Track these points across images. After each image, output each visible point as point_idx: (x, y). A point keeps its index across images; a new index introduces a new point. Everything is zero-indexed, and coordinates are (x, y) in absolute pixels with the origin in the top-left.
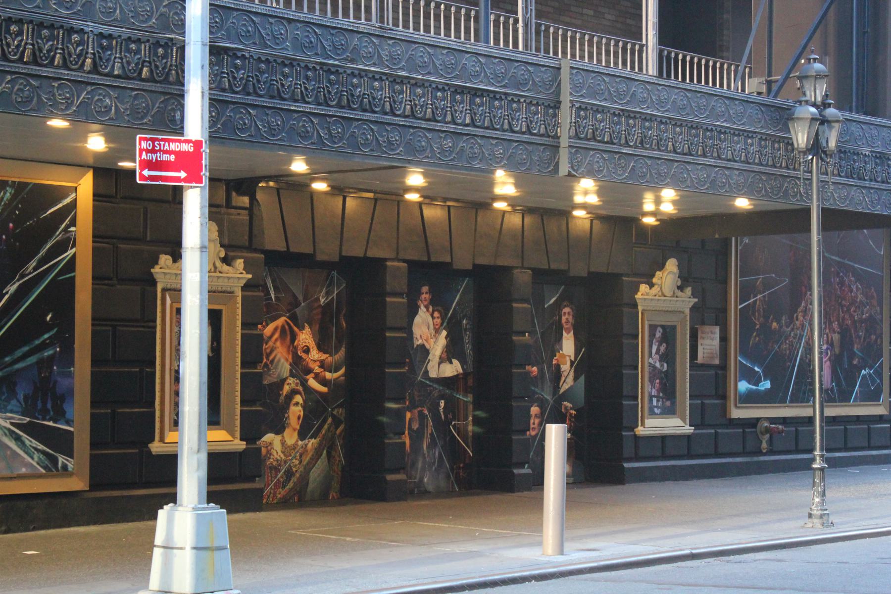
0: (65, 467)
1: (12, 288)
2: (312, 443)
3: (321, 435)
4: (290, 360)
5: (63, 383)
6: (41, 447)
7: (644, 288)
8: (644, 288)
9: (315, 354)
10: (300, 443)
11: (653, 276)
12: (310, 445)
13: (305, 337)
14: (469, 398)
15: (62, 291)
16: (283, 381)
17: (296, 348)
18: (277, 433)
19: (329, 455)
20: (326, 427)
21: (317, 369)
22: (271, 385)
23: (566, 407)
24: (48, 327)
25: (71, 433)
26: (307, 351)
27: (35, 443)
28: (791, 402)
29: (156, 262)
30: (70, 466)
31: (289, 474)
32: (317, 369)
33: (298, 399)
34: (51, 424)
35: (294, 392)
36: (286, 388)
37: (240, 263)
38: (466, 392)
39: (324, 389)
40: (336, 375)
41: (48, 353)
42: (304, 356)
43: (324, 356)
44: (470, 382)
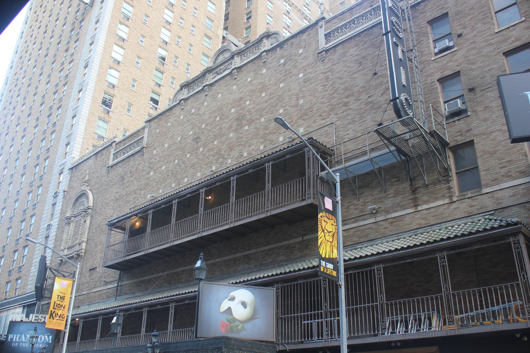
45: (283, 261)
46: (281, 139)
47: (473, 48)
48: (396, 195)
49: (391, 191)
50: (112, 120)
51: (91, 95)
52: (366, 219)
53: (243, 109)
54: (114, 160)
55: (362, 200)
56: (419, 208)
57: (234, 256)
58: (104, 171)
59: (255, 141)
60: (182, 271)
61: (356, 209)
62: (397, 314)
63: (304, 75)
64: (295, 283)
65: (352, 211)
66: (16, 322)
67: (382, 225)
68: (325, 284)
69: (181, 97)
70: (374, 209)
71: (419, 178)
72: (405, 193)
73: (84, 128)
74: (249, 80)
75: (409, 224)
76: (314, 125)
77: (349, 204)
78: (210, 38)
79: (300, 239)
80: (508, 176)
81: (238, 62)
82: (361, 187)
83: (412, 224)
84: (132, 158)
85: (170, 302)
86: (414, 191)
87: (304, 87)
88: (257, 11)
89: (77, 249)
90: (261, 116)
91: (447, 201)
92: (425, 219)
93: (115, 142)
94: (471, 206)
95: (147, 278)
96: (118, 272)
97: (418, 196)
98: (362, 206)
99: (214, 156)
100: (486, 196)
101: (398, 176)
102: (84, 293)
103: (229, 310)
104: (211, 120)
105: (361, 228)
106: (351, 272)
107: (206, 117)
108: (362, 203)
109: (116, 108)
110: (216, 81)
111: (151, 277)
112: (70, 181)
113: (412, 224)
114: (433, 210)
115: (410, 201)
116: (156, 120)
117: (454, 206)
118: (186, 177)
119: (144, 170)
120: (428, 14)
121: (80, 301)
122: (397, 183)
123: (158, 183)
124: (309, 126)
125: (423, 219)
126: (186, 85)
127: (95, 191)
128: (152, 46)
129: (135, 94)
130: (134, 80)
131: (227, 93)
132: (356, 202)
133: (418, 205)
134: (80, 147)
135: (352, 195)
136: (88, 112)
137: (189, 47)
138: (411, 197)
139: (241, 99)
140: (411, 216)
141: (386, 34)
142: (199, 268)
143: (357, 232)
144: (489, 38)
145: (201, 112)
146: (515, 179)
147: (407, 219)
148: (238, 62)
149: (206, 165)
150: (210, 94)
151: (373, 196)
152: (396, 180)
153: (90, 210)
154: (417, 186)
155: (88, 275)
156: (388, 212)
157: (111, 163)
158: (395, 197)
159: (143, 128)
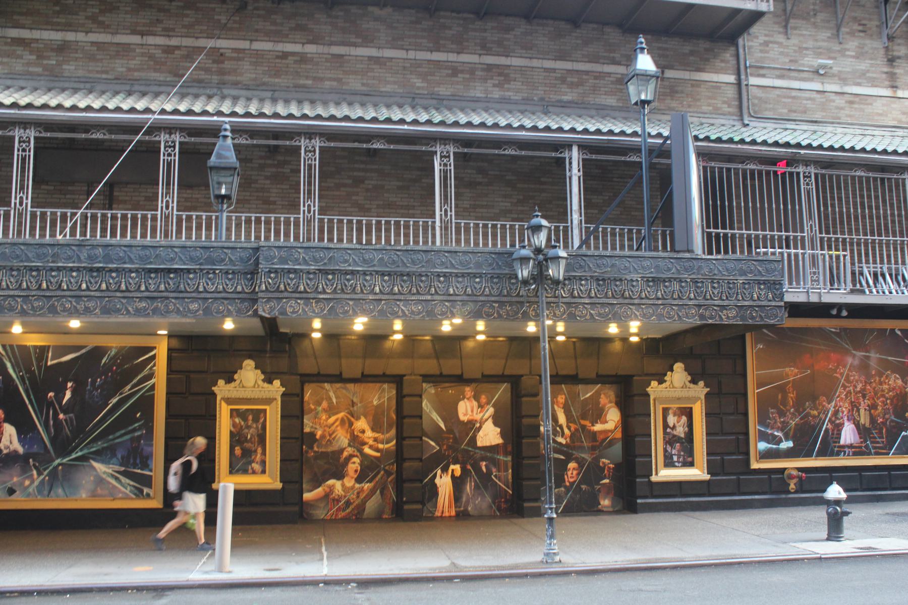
0: (148, 495)
1: (114, 400)
2: (367, 486)
3: (375, 481)
4: (349, 437)
5: (147, 449)
6: (132, 483)
7: (654, 384)
8: (654, 384)
9: (369, 434)
10: (357, 486)
11: (666, 375)
12: (366, 487)
13: (361, 424)
14: (509, 458)
15: (147, 402)
16: (342, 451)
17: (353, 431)
18: (338, 479)
19: (382, 493)
20: (379, 476)
21: (371, 442)
22: (333, 452)
23: (603, 463)
24: (138, 420)
25: (151, 476)
26: (363, 432)
27: (128, 481)
28: (817, 456)
29: (215, 384)
30: (152, 494)
31: (348, 503)
32: (371, 442)
33: (356, 460)
34: (139, 471)
35: (351, 456)
36: (345, 454)
37: (277, 383)
38: (506, 454)
39: (378, 454)
40: (387, 446)
41: (137, 434)
42: (360, 435)
43: (377, 435)
44: (510, 448)
45: (613, 108)
48: (860, 55)
49: (852, 45)
55: (794, 41)
57: (452, 57)
60: (235, 50)
61: (781, 53)
62: (882, 262)
64: (740, 166)
65: (771, 55)
67: (834, 101)
68: (808, 184)
70: (824, 67)
71: (899, 41)
72: (876, 59)
75: (881, 115)
77: (767, 39)
83: (887, 116)
85: (299, 134)
95: (56, 36)
97: (897, 71)
98: (795, 51)
101: (863, 22)
105: (794, 93)
106: (863, 174)
108: (794, 45)
111: (70, 36)
113: (887, 116)
115: (884, 76)
122: (862, 34)
125: (904, 113)
132: (781, 38)
133: (896, 87)
135: (775, 23)
138: (886, 70)
142: (645, 76)
143: (785, 97)
147: (878, 106)
151: (816, 40)
152: (861, 28)
154: (896, 53)
156: (844, 80)
158: (858, 58)
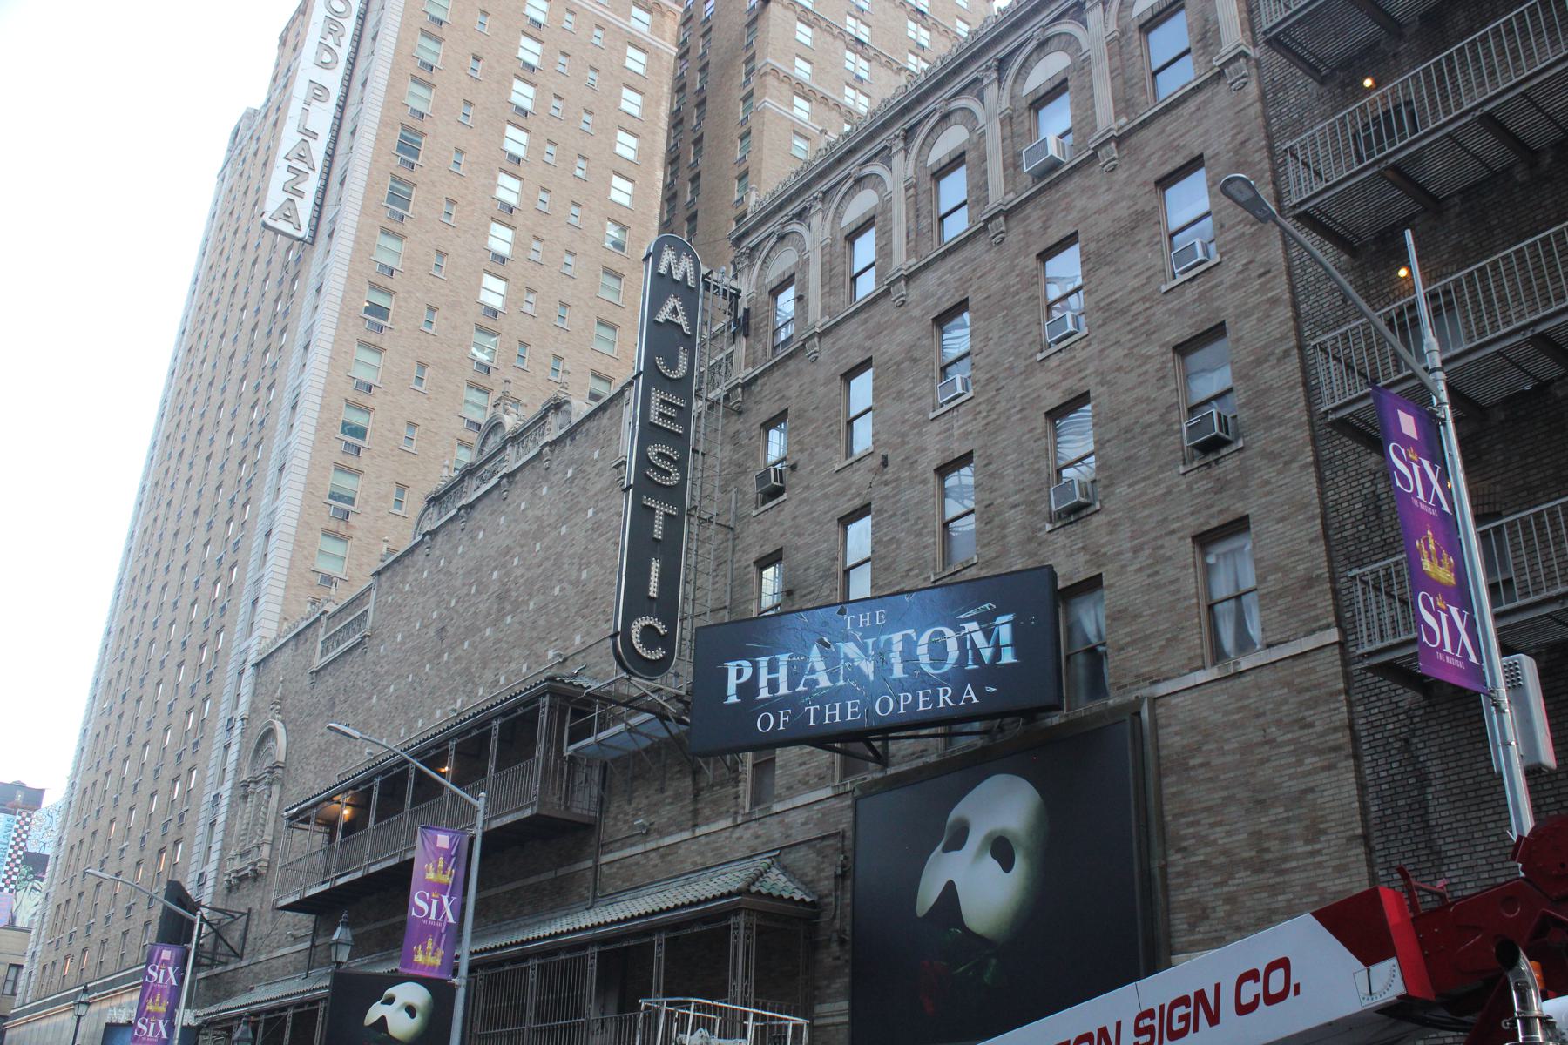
46: (551, 654)
47: (805, 501)
48: (677, 797)
50: (357, 534)
51: (303, 480)
52: (633, 845)
53: (508, 574)
54: (325, 652)
56: (698, 832)
58: (307, 681)
59: (516, 653)
63: (595, 513)
66: (117, 1025)
69: (428, 527)
73: (286, 563)
74: (523, 506)
76: (595, 631)
78: (619, 276)
79: (551, 875)
80: (806, 783)
81: (513, 459)
82: (634, 778)
84: (350, 658)
86: (696, 794)
87: (592, 541)
88: (759, 171)
89: (255, 859)
90: (531, 596)
91: (728, 822)
92: (701, 854)
93: (325, 612)
94: (757, 837)
96: (313, 917)
99: (460, 675)
100: (776, 818)
102: (262, 958)
103: (382, 1021)
104: (464, 591)
107: (458, 583)
109: (367, 502)
110: (479, 499)
112: (254, 694)
114: (713, 838)
116: (388, 574)
117: (738, 833)
118: (421, 716)
119: (363, 690)
120: (764, 407)
121: (257, 975)
123: (381, 721)
124: (588, 633)
126: (436, 500)
127: (290, 727)
128: (455, 328)
129: (413, 459)
130: (412, 425)
131: (497, 528)
134: (278, 609)
136: (295, 523)
137: (559, 311)
139: (509, 549)
140: (685, 846)
141: (626, 490)
144: (828, 481)
145: (453, 570)
146: (813, 788)
148: (513, 459)
149: (450, 693)
150: (469, 526)
153: (279, 771)
155: (269, 917)
156: (662, 833)
157: (318, 662)
159: (369, 589)
